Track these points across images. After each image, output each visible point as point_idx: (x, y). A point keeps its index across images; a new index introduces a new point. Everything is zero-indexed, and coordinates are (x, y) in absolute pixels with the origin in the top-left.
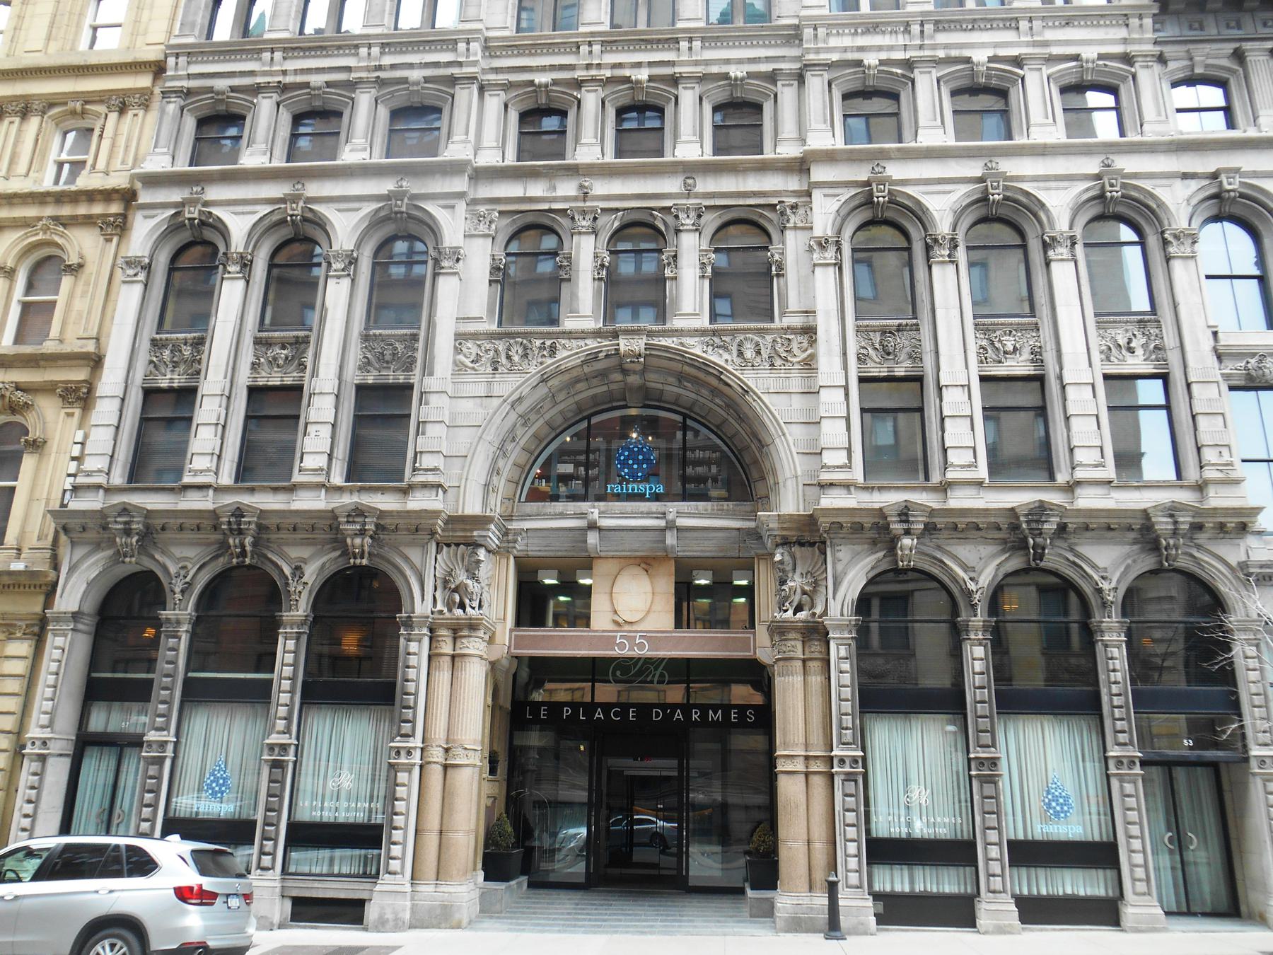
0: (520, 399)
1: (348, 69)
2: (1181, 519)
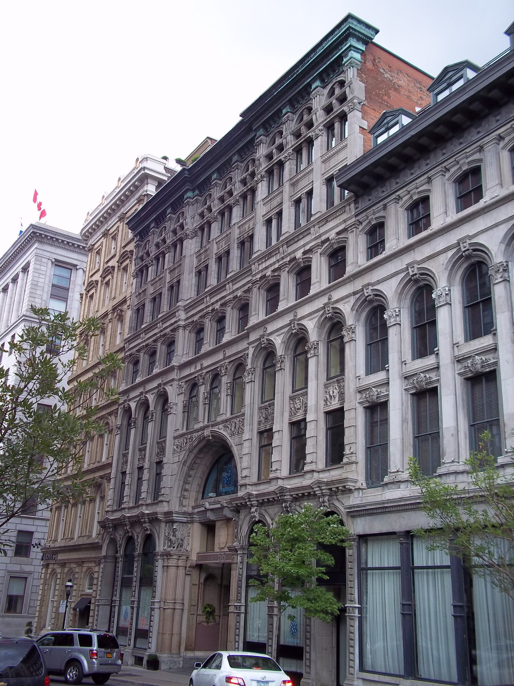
0: (185, 462)
1: (155, 334)
2: (323, 488)
